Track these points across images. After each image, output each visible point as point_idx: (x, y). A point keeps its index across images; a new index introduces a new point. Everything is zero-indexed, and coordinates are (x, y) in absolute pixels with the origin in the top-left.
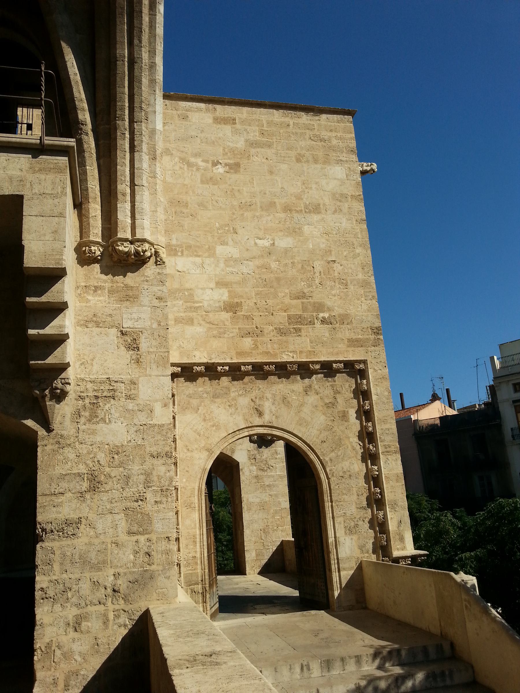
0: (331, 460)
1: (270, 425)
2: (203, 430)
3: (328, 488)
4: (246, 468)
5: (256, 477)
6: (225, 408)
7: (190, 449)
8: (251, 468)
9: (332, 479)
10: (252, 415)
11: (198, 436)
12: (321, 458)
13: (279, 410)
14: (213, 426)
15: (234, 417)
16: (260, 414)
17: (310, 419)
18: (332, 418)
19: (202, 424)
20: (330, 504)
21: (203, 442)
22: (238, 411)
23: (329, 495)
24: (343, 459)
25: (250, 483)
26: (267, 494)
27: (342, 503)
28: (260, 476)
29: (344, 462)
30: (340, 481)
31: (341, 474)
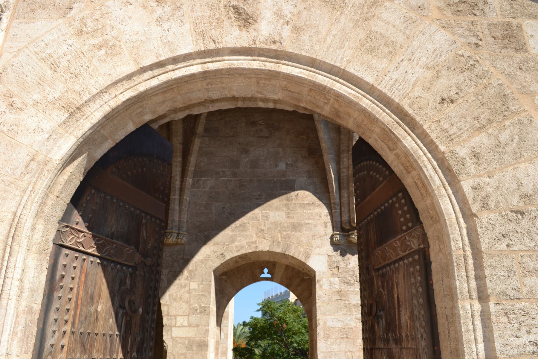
0: (476, 155)
1: (273, 47)
2: (69, 57)
3: (468, 249)
4: (324, 280)
5: (339, 292)
6: (145, 7)
7: (18, 105)
8: (332, 279)
9: (484, 218)
10: (219, 21)
11: (49, 72)
12: (442, 148)
13: (305, 13)
14: (100, 47)
15: (166, 26)
16: (246, 19)
17: (401, 39)
18: (473, 40)
19: (70, 42)
20: (477, 306)
21: (62, 85)
22: (180, 13)
23: (472, 273)
24: (517, 157)
25: (330, 300)
26: (353, 317)
27: (525, 304)
28: (345, 291)
29: (522, 166)
30: (511, 227)
31: (515, 202)
